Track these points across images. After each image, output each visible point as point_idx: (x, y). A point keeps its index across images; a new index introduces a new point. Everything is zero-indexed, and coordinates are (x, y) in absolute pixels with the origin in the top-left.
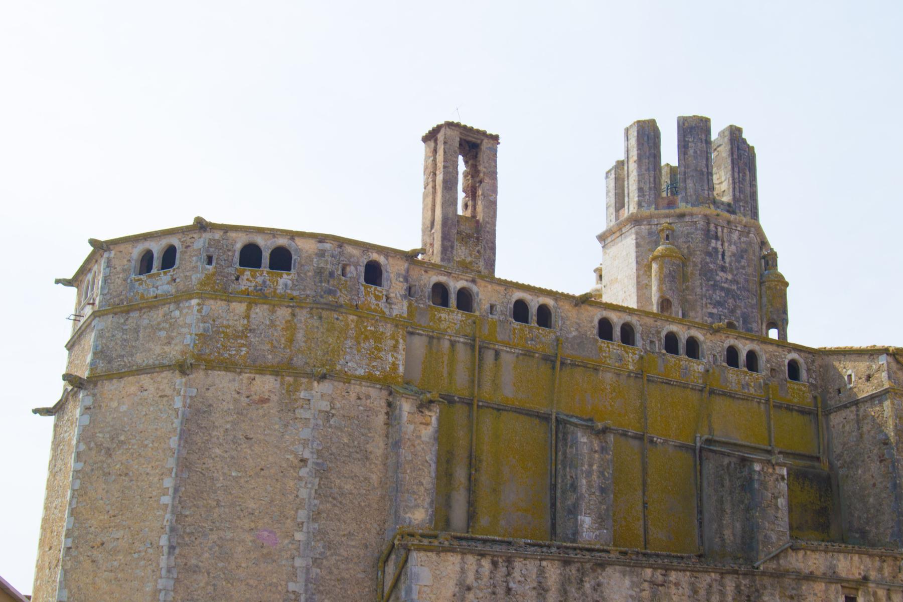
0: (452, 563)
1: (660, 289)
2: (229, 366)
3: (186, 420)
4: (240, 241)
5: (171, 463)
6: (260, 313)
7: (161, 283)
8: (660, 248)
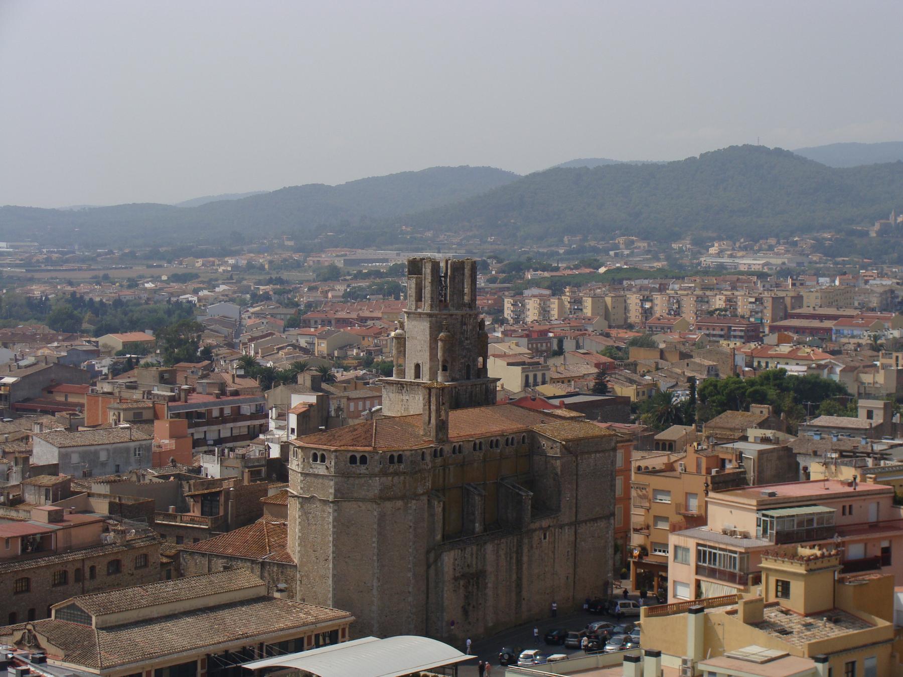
0: (452, 553)
1: (443, 355)
2: (389, 499)
3: (379, 520)
4: (389, 455)
5: (375, 533)
6: (396, 478)
7: (363, 469)
8: (442, 334)
